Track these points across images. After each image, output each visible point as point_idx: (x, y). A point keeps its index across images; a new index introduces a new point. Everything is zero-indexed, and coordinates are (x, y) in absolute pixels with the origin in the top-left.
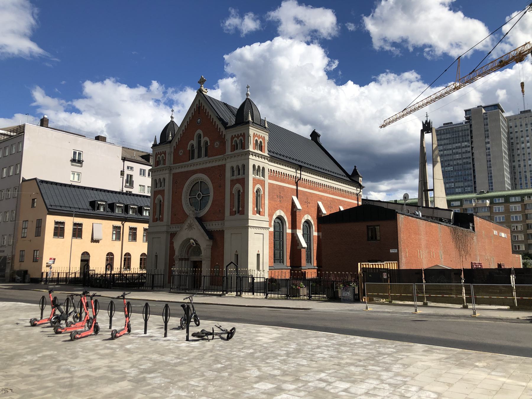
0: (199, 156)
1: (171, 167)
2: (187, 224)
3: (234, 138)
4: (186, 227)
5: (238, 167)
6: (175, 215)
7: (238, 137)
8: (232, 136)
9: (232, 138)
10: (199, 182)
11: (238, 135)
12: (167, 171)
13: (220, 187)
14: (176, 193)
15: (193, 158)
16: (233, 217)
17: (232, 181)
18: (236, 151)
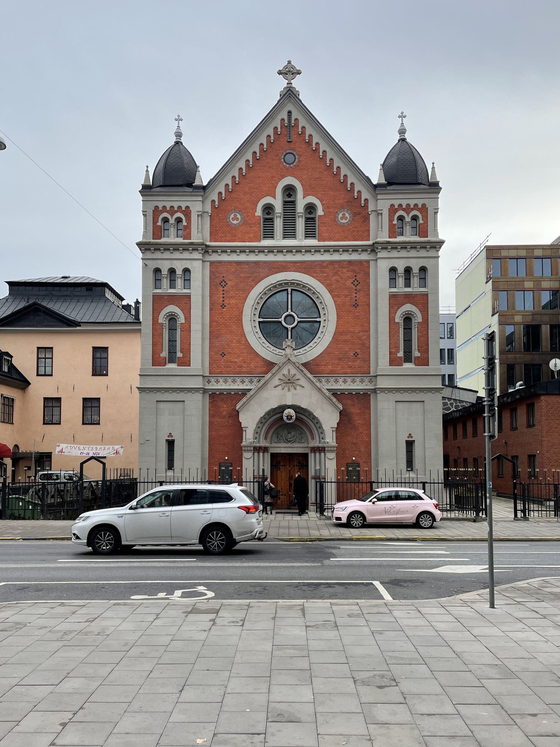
0: (290, 232)
1: (207, 246)
2: (280, 376)
3: (396, 211)
4: (276, 381)
5: (408, 270)
6: (223, 355)
7: (408, 209)
8: (392, 206)
9: (393, 210)
10: (289, 290)
11: (408, 205)
12: (197, 255)
13: (356, 306)
14: (223, 306)
15: (269, 233)
16: (396, 370)
17: (393, 297)
18: (399, 239)
